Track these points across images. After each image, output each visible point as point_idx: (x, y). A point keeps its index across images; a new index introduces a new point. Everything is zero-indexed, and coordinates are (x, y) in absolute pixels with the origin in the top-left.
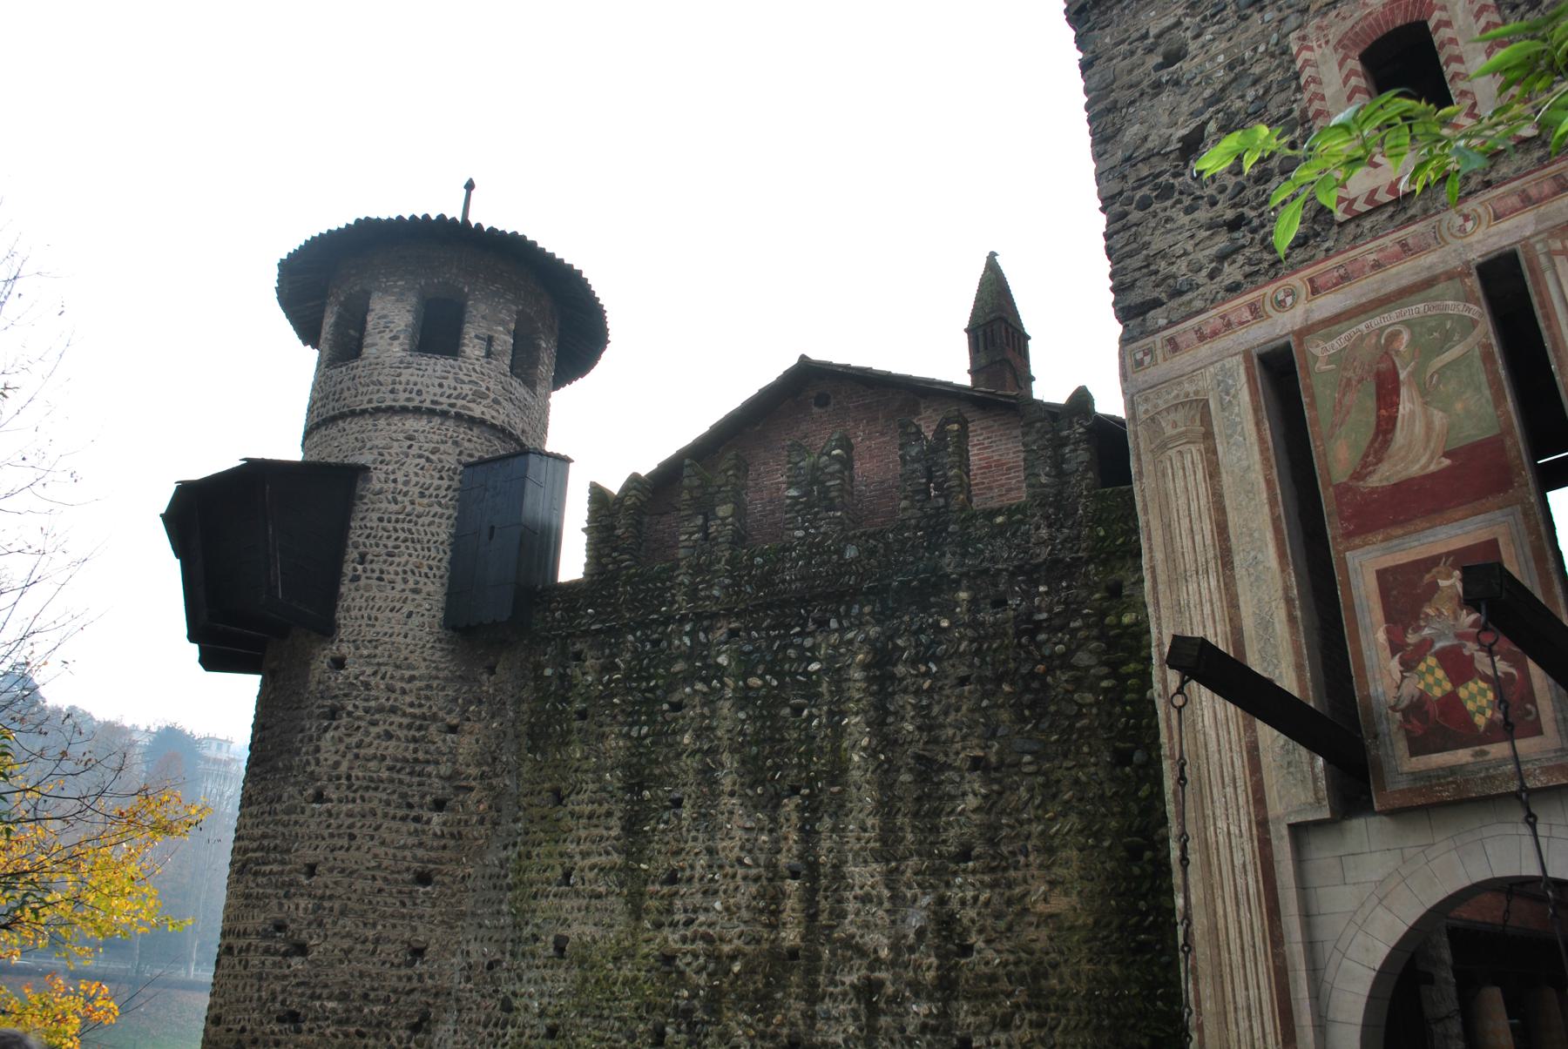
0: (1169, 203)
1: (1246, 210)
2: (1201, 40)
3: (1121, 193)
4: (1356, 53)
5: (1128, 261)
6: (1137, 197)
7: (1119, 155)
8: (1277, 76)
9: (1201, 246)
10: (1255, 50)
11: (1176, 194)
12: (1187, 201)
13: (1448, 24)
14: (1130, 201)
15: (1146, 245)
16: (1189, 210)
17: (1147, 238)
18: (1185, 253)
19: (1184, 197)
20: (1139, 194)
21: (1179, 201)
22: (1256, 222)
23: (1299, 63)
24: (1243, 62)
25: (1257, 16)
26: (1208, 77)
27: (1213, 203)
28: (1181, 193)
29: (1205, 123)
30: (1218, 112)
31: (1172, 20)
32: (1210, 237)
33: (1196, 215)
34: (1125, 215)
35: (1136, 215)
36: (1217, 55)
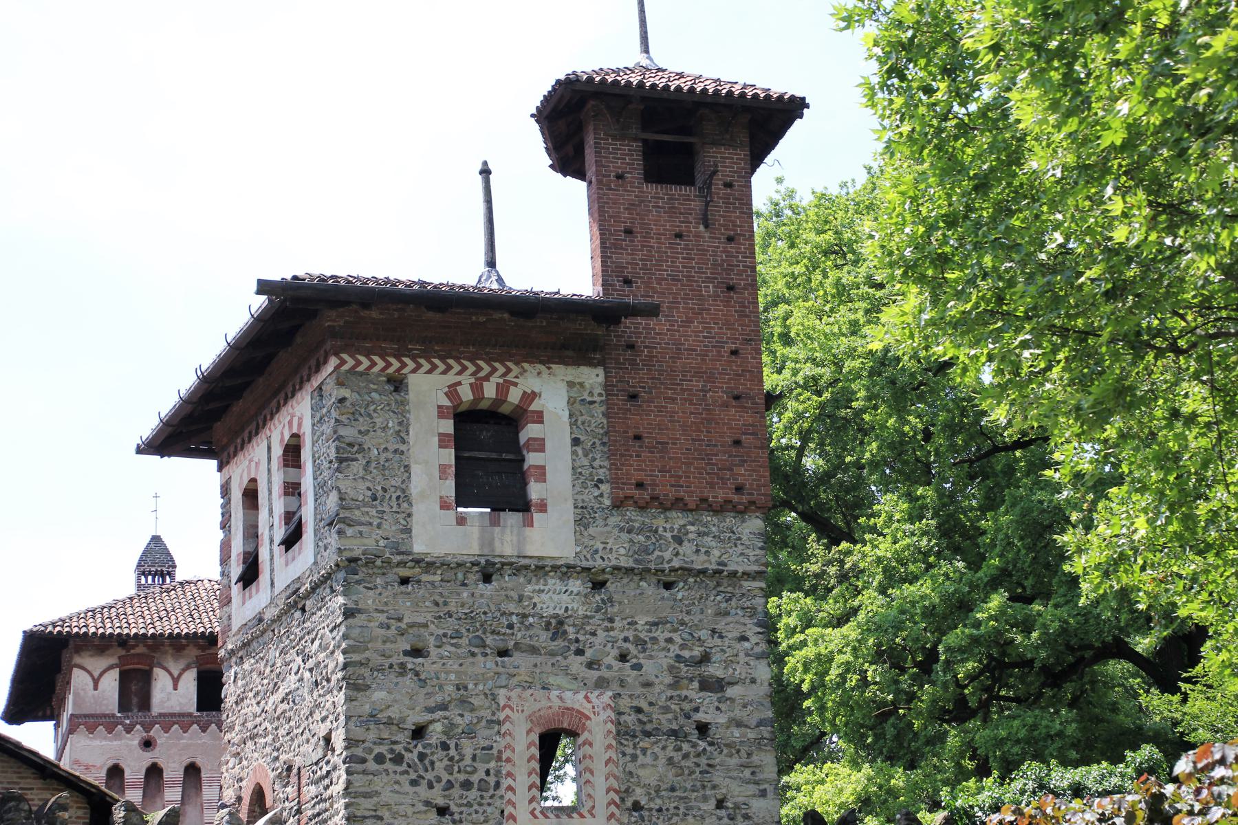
0: (399, 769)
1: (451, 803)
2: (440, 650)
3: (363, 742)
4: (538, 730)
5: (361, 800)
6: (376, 751)
7: (367, 708)
8: (487, 714)
9: (418, 816)
10: (476, 685)
11: (405, 764)
12: (413, 776)
13: (591, 745)
14: (370, 751)
15: (377, 793)
16: (414, 783)
17: (378, 788)
18: (406, 816)
19: (411, 771)
20: (377, 750)
21: (407, 772)
22: (457, 817)
23: (502, 716)
24: (466, 688)
25: (480, 658)
26: (441, 687)
27: (431, 786)
28: (409, 766)
29: (431, 722)
30: (446, 718)
31: (421, 620)
32: (425, 812)
33: (417, 789)
34: (364, 761)
35: (372, 765)
36: (451, 672)
